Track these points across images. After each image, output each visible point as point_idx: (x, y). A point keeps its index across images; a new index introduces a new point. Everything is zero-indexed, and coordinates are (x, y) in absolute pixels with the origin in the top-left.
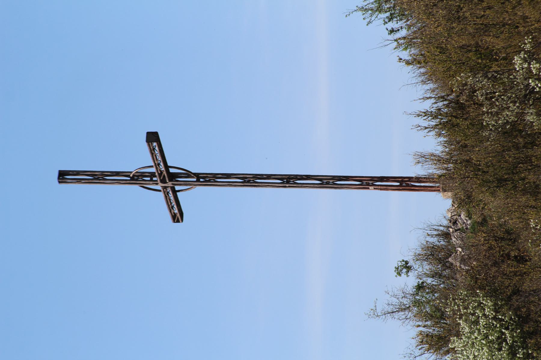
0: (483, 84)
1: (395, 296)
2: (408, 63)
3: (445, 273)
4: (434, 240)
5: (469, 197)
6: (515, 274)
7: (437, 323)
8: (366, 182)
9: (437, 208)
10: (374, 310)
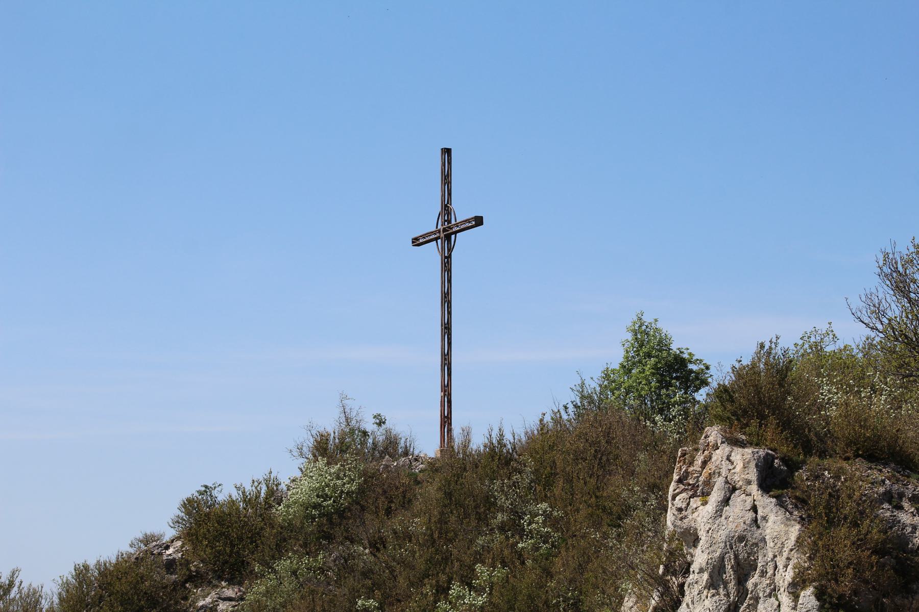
0: (526, 479)
1: (357, 414)
2: (541, 420)
3: (376, 452)
4: (402, 444)
5: (437, 470)
6: (376, 507)
7: (337, 447)
8: (446, 390)
9: (428, 445)
10: (346, 398)
